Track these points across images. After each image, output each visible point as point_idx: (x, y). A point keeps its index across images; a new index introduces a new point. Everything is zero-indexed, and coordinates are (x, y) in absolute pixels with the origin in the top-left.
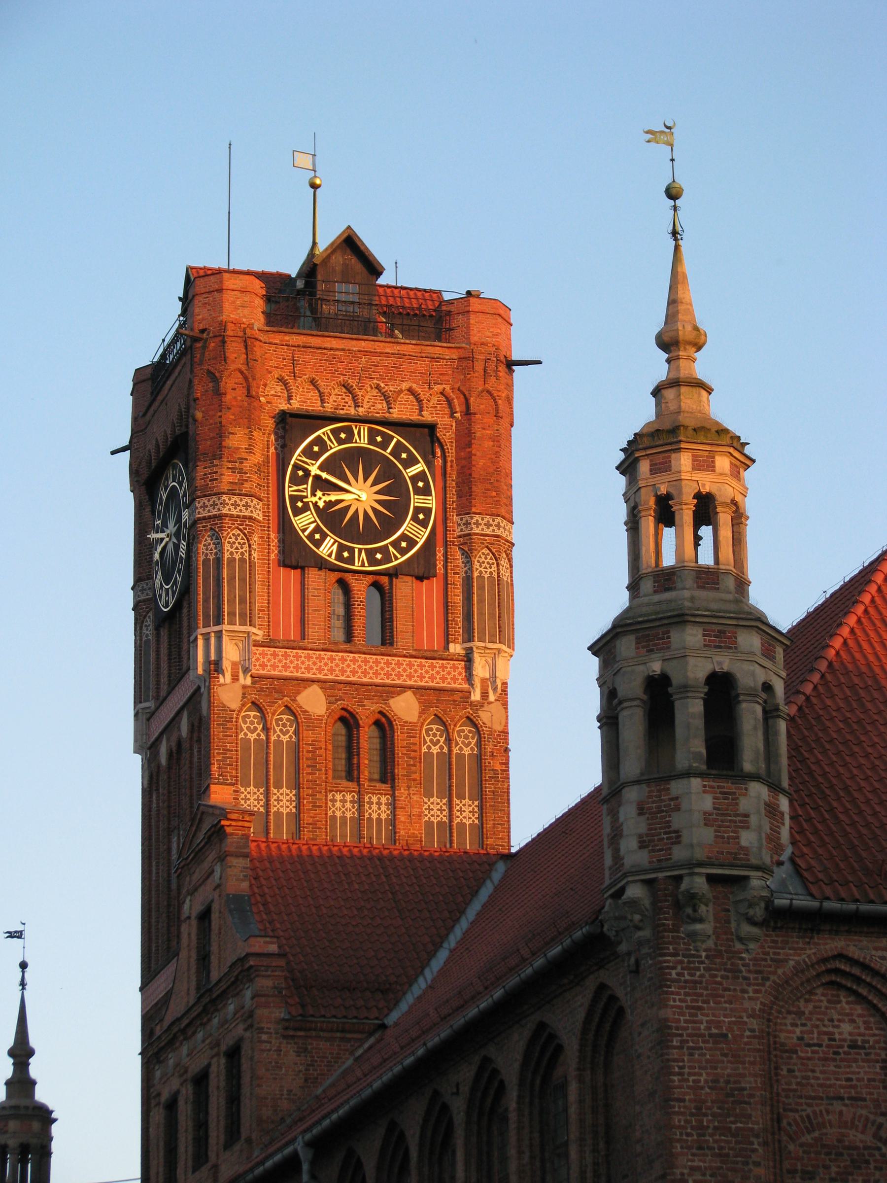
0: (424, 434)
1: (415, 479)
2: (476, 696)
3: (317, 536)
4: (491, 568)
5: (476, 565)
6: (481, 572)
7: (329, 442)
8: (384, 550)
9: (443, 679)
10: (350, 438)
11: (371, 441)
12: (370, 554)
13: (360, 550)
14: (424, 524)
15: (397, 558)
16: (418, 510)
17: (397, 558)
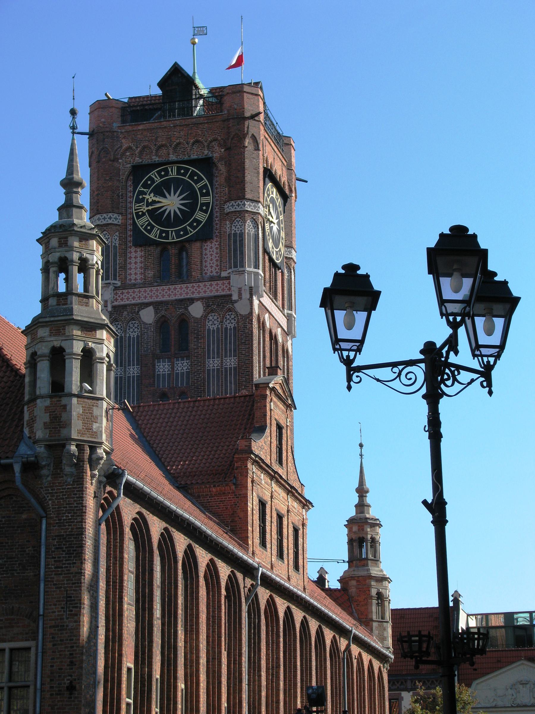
0: (206, 164)
1: (201, 189)
2: (235, 297)
3: (149, 228)
4: (241, 227)
5: (233, 228)
6: (235, 231)
7: (155, 179)
8: (185, 229)
9: (217, 290)
10: (167, 173)
11: (178, 173)
12: (177, 232)
13: (172, 231)
14: (206, 212)
15: (191, 232)
16: (202, 205)
17: (191, 232)
